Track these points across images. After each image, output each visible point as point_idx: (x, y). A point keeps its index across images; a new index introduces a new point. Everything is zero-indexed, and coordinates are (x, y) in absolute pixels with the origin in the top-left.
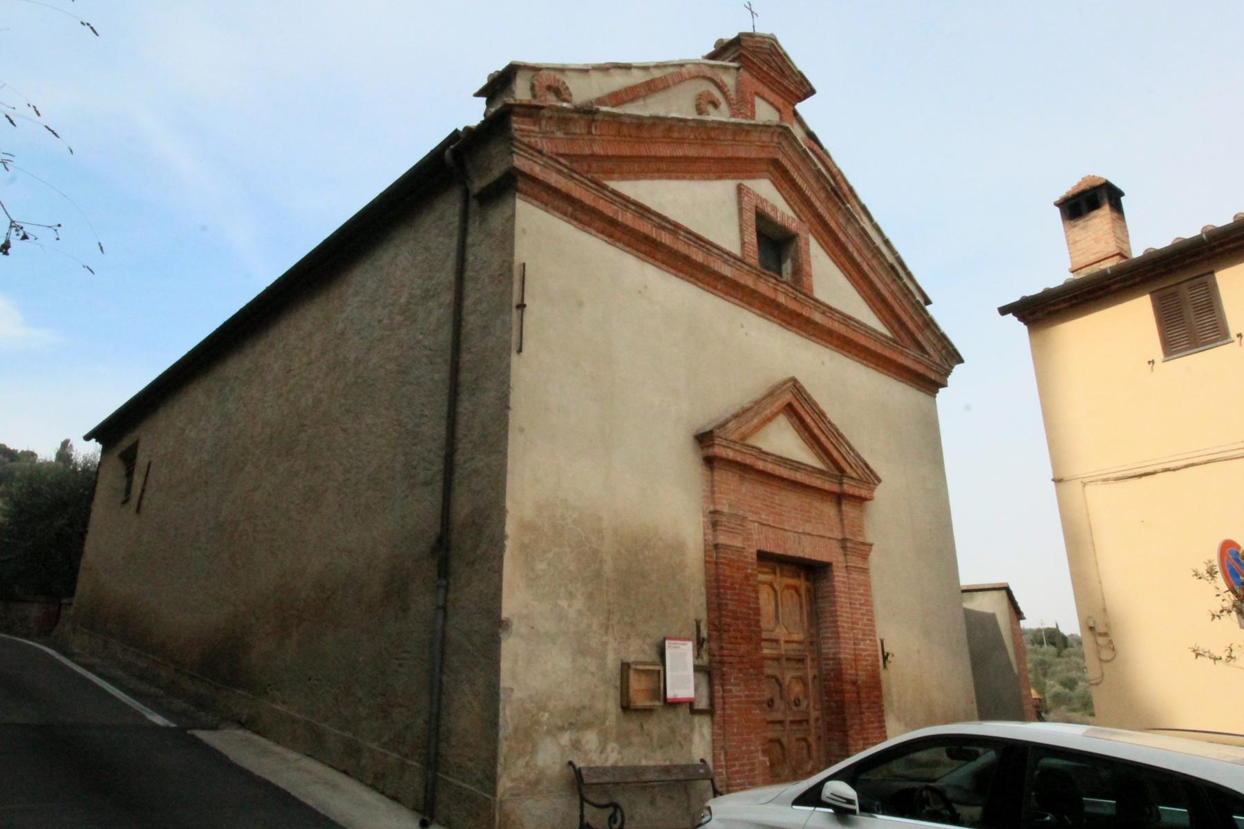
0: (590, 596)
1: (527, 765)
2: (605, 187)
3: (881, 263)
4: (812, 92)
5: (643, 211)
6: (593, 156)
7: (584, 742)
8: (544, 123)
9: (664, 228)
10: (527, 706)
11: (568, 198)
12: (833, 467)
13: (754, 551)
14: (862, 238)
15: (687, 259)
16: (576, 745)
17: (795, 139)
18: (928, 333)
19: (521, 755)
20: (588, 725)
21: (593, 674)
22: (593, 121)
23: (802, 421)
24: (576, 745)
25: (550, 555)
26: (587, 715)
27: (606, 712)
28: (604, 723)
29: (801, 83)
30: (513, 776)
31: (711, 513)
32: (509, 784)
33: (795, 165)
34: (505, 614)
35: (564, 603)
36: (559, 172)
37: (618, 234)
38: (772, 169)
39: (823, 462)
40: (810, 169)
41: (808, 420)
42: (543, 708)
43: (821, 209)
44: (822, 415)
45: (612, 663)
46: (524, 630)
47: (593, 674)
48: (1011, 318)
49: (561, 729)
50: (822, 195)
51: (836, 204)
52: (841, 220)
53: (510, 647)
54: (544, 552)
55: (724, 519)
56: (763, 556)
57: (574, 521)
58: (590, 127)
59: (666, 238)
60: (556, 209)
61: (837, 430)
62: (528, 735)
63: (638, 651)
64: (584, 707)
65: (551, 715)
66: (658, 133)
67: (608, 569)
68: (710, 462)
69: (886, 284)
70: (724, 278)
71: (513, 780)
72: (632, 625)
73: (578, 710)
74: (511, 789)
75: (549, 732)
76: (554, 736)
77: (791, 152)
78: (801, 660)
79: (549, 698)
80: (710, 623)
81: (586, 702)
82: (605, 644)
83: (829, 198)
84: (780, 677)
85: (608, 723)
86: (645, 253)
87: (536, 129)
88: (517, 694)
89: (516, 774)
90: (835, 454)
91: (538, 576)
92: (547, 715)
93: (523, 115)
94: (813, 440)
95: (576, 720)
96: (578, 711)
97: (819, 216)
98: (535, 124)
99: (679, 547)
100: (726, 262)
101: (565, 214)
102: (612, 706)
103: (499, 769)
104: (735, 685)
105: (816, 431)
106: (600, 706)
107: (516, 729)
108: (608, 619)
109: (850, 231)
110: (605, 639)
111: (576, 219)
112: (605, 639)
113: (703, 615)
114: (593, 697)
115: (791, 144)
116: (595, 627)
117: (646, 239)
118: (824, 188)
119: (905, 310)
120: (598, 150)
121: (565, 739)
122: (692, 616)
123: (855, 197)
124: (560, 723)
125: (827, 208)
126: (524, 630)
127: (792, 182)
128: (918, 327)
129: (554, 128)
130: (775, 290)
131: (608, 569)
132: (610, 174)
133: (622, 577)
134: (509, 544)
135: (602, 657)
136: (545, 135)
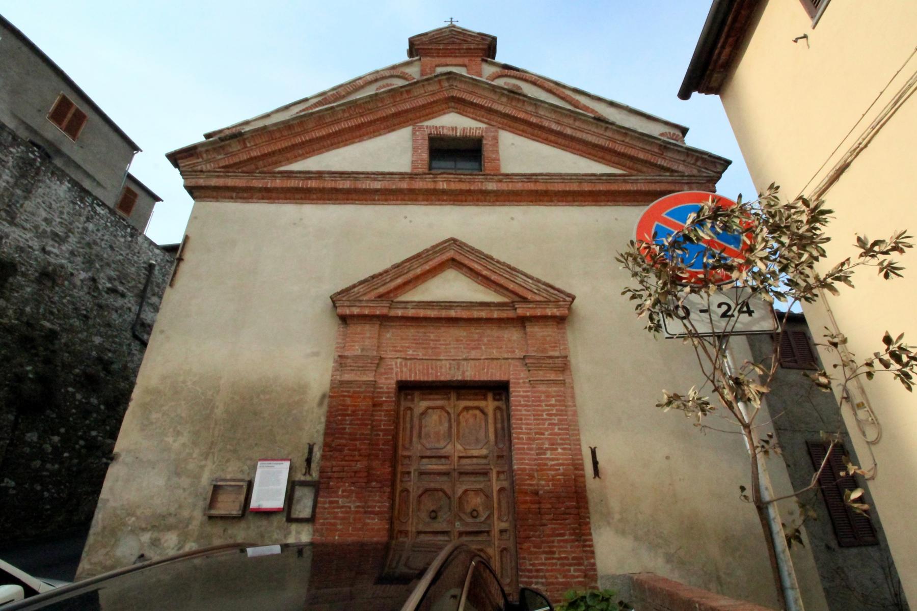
0: (197, 433)
1: (107, 554)
2: (275, 173)
3: (584, 121)
4: (494, 39)
5: (320, 175)
6: (252, 159)
7: (163, 541)
8: (205, 156)
9: (310, 178)
10: (119, 512)
12: (514, 296)
13: (393, 382)
14: (555, 112)
15: (336, 190)
16: (155, 543)
17: (462, 76)
18: (670, 154)
19: (104, 546)
20: (169, 528)
21: (184, 490)
22: (244, 141)
23: (471, 270)
24: (155, 543)
25: (165, 408)
26: (172, 520)
27: (191, 518)
28: (187, 526)
29: (483, 39)
30: (92, 561)
32: (87, 566)
33: (471, 93)
34: (116, 450)
35: (170, 440)
36: (218, 177)
37: (234, 195)
38: (453, 104)
39: (505, 296)
40: (484, 89)
41: (476, 266)
42: (133, 514)
43: (508, 110)
44: (489, 258)
46: (129, 459)
47: (184, 490)
48: (695, 95)
49: (143, 530)
50: (504, 100)
51: (519, 100)
52: (530, 108)
53: (113, 471)
54: (162, 406)
55: (349, 361)
56: (406, 388)
57: (194, 383)
58: (245, 143)
59: (312, 184)
60: (225, 198)
61: (509, 266)
62: (113, 532)
63: (233, 471)
64: (170, 514)
65: (138, 518)
66: (311, 125)
67: (219, 412)
68: (344, 319)
69: (599, 135)
70: (376, 191)
71: (91, 564)
72: (235, 451)
73: (164, 516)
74: (88, 570)
75: (132, 531)
76: (137, 535)
77: (463, 86)
79: (138, 507)
80: (326, 445)
81: (172, 510)
82: (202, 468)
83: (511, 99)
84: (449, 492)
85: (190, 527)
86: (302, 199)
87: (200, 160)
88: (112, 504)
89: (94, 560)
90: (511, 286)
91: (152, 423)
92: (133, 519)
93: (186, 157)
94: (487, 282)
95: (159, 523)
96: (164, 517)
97: (506, 116)
98: (198, 158)
99: (302, 389)
100: (375, 179)
101: (232, 198)
102: (198, 516)
103: (84, 555)
104: (343, 497)
105: (485, 272)
106: (186, 513)
107: (104, 528)
108: (210, 448)
109: (542, 112)
110: (203, 463)
111: (241, 198)
112: (203, 463)
113: (319, 440)
114: (180, 507)
115: (461, 81)
116: (195, 456)
117: (297, 190)
118: (503, 94)
119: (633, 147)
120: (254, 154)
121: (146, 537)
122: (305, 440)
123: (564, 87)
124: (144, 526)
125: (515, 108)
126: (129, 459)
127: (472, 104)
128: (654, 154)
129: (215, 155)
130: (435, 182)
131: (219, 412)
132: (278, 163)
133: (244, 420)
134: (132, 405)
135: (198, 477)
136: (208, 161)
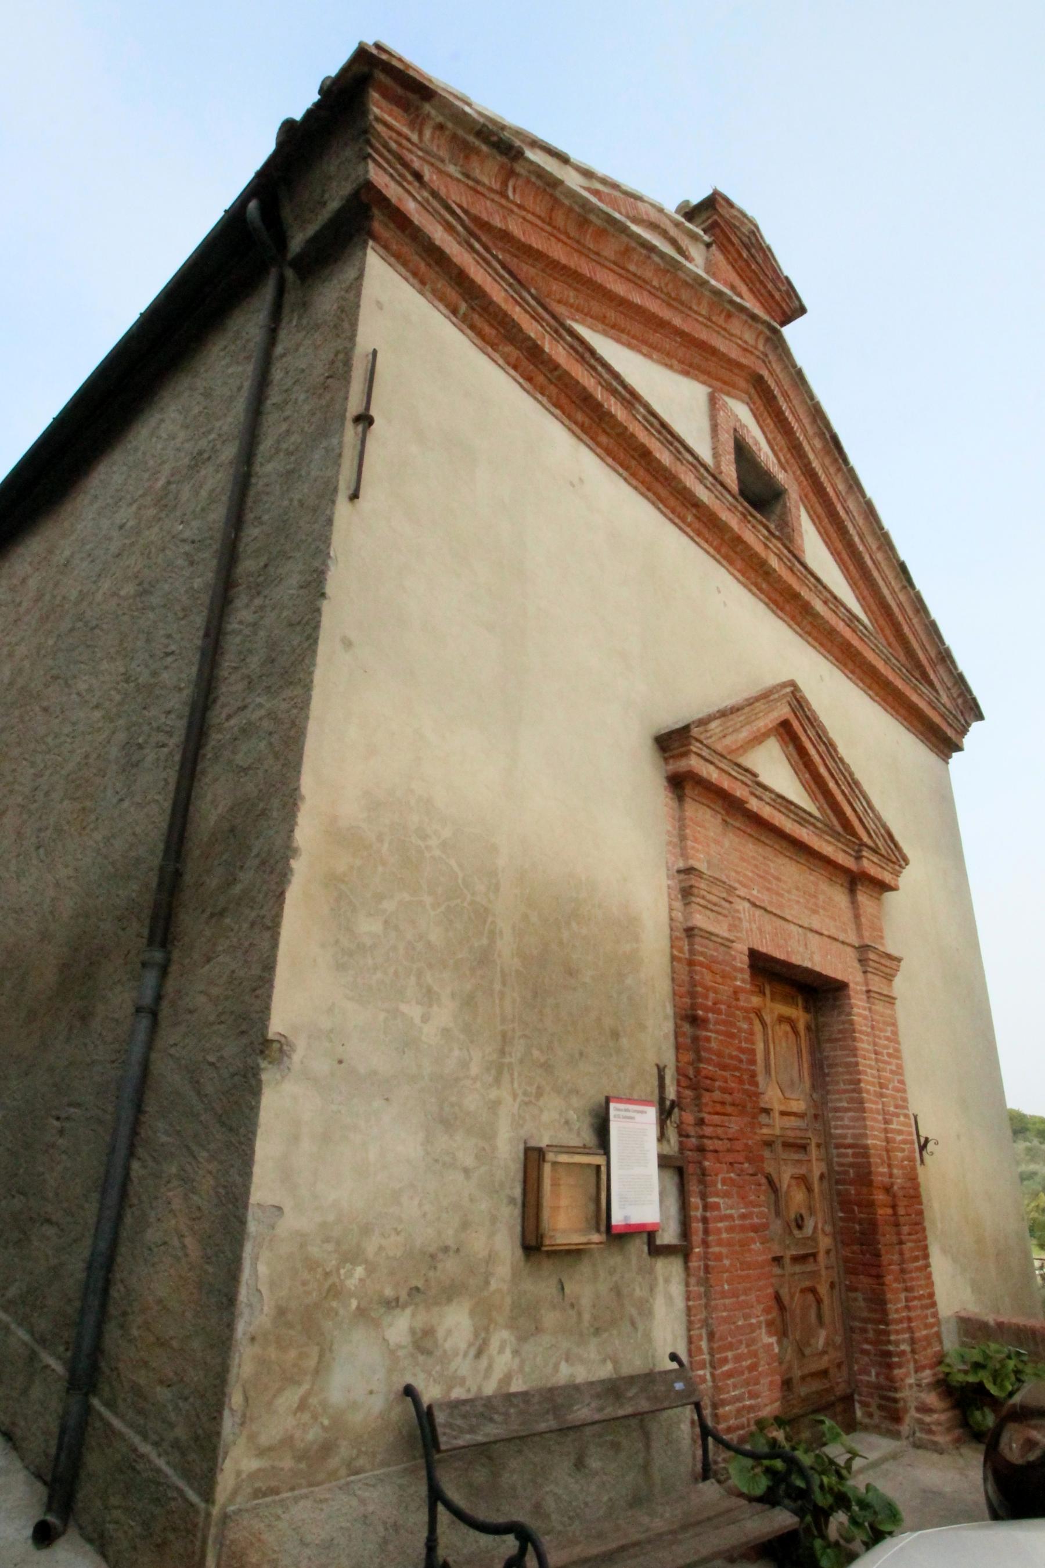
0: (469, 1002)
1: (302, 1406)
4: (802, 310)
6: (505, 236)
7: (440, 1334)
9: (614, 392)
11: (460, 279)
15: (645, 454)
16: (424, 1342)
18: (941, 669)
19: (290, 1380)
20: (451, 1292)
21: (466, 1171)
22: (512, 173)
23: (802, 751)
24: (424, 1342)
25: (389, 905)
26: (450, 1266)
27: (491, 1259)
30: (264, 1440)
31: (679, 872)
32: (251, 1464)
34: (277, 1025)
35: (414, 1011)
36: (449, 228)
42: (352, 1257)
44: (830, 747)
45: (507, 1152)
46: (321, 1066)
49: (392, 1304)
51: (836, 461)
52: (841, 487)
53: (282, 1104)
54: (379, 897)
55: (703, 885)
57: (444, 845)
61: (851, 774)
62: (307, 1323)
63: (557, 1125)
64: (446, 1249)
65: (371, 1269)
66: (610, 249)
67: (505, 947)
68: (679, 784)
69: (893, 592)
70: (696, 504)
71: (262, 1452)
72: (547, 1067)
73: (433, 1257)
74: (253, 1476)
76: (376, 1324)
78: (803, 1148)
79: (366, 1230)
81: (449, 1237)
82: (494, 1106)
84: (775, 1176)
85: (494, 1285)
86: (582, 427)
88: (291, 1222)
89: (271, 1432)
92: (360, 1271)
94: (816, 784)
95: (426, 1281)
99: (627, 925)
100: (701, 480)
101: (454, 312)
102: (505, 1245)
104: (726, 1195)
105: (822, 770)
106: (478, 1244)
107: (281, 1312)
108: (502, 1053)
110: (494, 1094)
111: (472, 327)
112: (494, 1094)
113: (669, 1058)
114: (465, 1225)
115: (780, 359)
116: (474, 1070)
119: (915, 634)
121: (399, 1328)
122: (651, 1058)
124: (389, 1292)
128: (930, 660)
130: (766, 546)
133: (526, 973)
134: (301, 870)
135: (488, 1135)
